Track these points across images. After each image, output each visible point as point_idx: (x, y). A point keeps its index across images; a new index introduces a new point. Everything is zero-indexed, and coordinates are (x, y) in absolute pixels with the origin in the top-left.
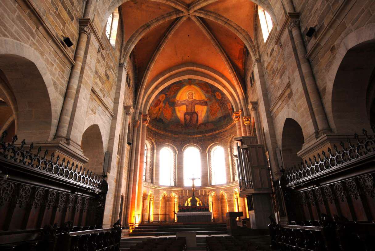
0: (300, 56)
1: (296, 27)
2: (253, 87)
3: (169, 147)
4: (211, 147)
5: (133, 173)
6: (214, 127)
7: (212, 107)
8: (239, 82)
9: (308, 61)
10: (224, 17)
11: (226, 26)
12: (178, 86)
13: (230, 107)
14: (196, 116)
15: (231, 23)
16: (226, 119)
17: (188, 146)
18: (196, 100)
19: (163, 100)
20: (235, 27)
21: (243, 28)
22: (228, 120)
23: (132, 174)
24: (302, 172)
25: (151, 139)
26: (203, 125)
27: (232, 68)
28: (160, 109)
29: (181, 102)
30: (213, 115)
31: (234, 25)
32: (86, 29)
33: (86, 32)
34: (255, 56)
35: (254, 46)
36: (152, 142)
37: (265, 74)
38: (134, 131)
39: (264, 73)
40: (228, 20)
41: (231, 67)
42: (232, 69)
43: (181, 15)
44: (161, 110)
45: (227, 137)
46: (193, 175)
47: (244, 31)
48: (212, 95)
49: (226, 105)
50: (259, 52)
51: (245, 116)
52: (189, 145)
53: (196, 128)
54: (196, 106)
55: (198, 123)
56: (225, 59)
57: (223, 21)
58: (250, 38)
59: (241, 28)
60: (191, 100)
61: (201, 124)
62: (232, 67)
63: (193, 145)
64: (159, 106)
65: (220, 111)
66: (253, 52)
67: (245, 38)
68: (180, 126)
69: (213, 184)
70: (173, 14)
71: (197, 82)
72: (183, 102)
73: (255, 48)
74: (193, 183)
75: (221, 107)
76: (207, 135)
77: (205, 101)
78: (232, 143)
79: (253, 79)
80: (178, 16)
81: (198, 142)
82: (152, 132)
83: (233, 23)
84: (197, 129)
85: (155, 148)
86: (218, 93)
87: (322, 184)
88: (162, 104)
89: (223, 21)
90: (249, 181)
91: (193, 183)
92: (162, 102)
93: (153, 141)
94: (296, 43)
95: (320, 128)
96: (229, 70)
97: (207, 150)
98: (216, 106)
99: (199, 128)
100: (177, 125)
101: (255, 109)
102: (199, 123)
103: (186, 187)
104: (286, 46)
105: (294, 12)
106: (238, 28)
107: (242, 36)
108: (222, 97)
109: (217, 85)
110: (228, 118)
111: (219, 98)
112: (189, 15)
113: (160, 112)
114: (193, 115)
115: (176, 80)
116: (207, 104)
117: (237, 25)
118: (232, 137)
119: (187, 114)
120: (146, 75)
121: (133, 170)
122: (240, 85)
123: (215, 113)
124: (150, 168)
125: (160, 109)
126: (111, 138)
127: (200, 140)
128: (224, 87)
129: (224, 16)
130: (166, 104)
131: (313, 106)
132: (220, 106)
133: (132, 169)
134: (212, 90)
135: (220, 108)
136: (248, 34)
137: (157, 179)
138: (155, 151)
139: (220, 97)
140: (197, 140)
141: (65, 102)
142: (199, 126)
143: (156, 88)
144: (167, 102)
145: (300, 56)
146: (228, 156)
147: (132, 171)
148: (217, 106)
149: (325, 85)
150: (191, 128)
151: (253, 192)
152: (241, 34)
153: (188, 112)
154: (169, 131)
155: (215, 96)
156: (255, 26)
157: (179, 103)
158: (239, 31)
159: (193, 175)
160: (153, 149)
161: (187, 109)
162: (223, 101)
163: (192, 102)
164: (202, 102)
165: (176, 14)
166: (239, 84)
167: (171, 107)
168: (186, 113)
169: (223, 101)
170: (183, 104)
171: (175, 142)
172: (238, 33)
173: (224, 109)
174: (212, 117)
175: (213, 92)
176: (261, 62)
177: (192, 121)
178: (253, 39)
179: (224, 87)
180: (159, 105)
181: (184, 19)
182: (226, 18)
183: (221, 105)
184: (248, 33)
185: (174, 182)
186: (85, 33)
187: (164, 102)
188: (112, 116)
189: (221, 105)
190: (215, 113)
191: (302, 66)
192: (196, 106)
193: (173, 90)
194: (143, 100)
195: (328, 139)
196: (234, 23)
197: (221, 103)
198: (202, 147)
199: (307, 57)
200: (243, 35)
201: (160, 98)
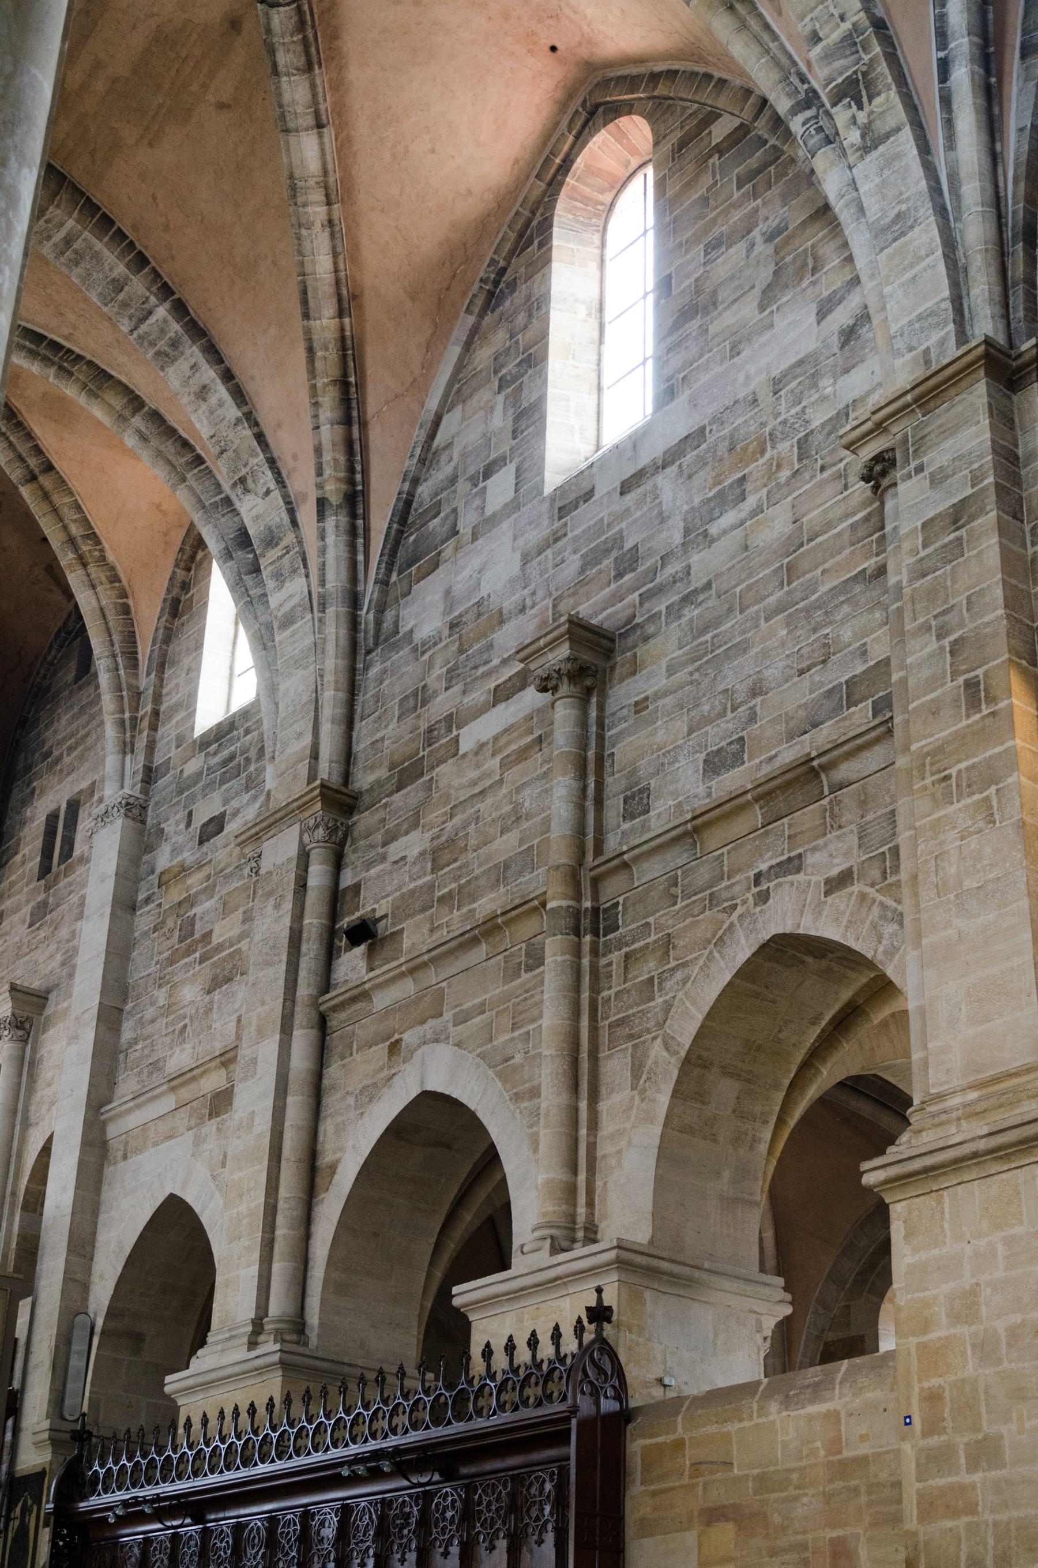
0: (304, 990)
2: (47, 888)
9: (322, 1024)
10: (29, 436)
11: (26, 492)
15: (56, 498)
20: (75, 530)
21: (111, 557)
24: (159, 1460)
31: (69, 515)
34: (124, 753)
35: (137, 695)
39: (141, 897)
40: (49, 468)
47: (115, 578)
50: (151, 747)
57: (22, 459)
58: (131, 638)
59: (102, 551)
66: (121, 723)
67: (106, 623)
73: (137, 710)
79: (69, 843)
83: (68, 500)
87: (213, 1517)
89: (22, 459)
94: (306, 921)
101: (20, 1033)
104: (271, 902)
105: (343, 789)
106: (85, 548)
107: (94, 603)
117: (87, 520)
129: (37, 430)
131: (280, 1220)
136: (126, 610)
149: (338, 1155)
152: (94, 587)
156: (176, 591)
158: (85, 565)
172: (81, 572)
176: (143, 822)
178: (145, 650)
182: (38, 450)
184: (130, 602)
196: (78, 508)
200: (98, 599)
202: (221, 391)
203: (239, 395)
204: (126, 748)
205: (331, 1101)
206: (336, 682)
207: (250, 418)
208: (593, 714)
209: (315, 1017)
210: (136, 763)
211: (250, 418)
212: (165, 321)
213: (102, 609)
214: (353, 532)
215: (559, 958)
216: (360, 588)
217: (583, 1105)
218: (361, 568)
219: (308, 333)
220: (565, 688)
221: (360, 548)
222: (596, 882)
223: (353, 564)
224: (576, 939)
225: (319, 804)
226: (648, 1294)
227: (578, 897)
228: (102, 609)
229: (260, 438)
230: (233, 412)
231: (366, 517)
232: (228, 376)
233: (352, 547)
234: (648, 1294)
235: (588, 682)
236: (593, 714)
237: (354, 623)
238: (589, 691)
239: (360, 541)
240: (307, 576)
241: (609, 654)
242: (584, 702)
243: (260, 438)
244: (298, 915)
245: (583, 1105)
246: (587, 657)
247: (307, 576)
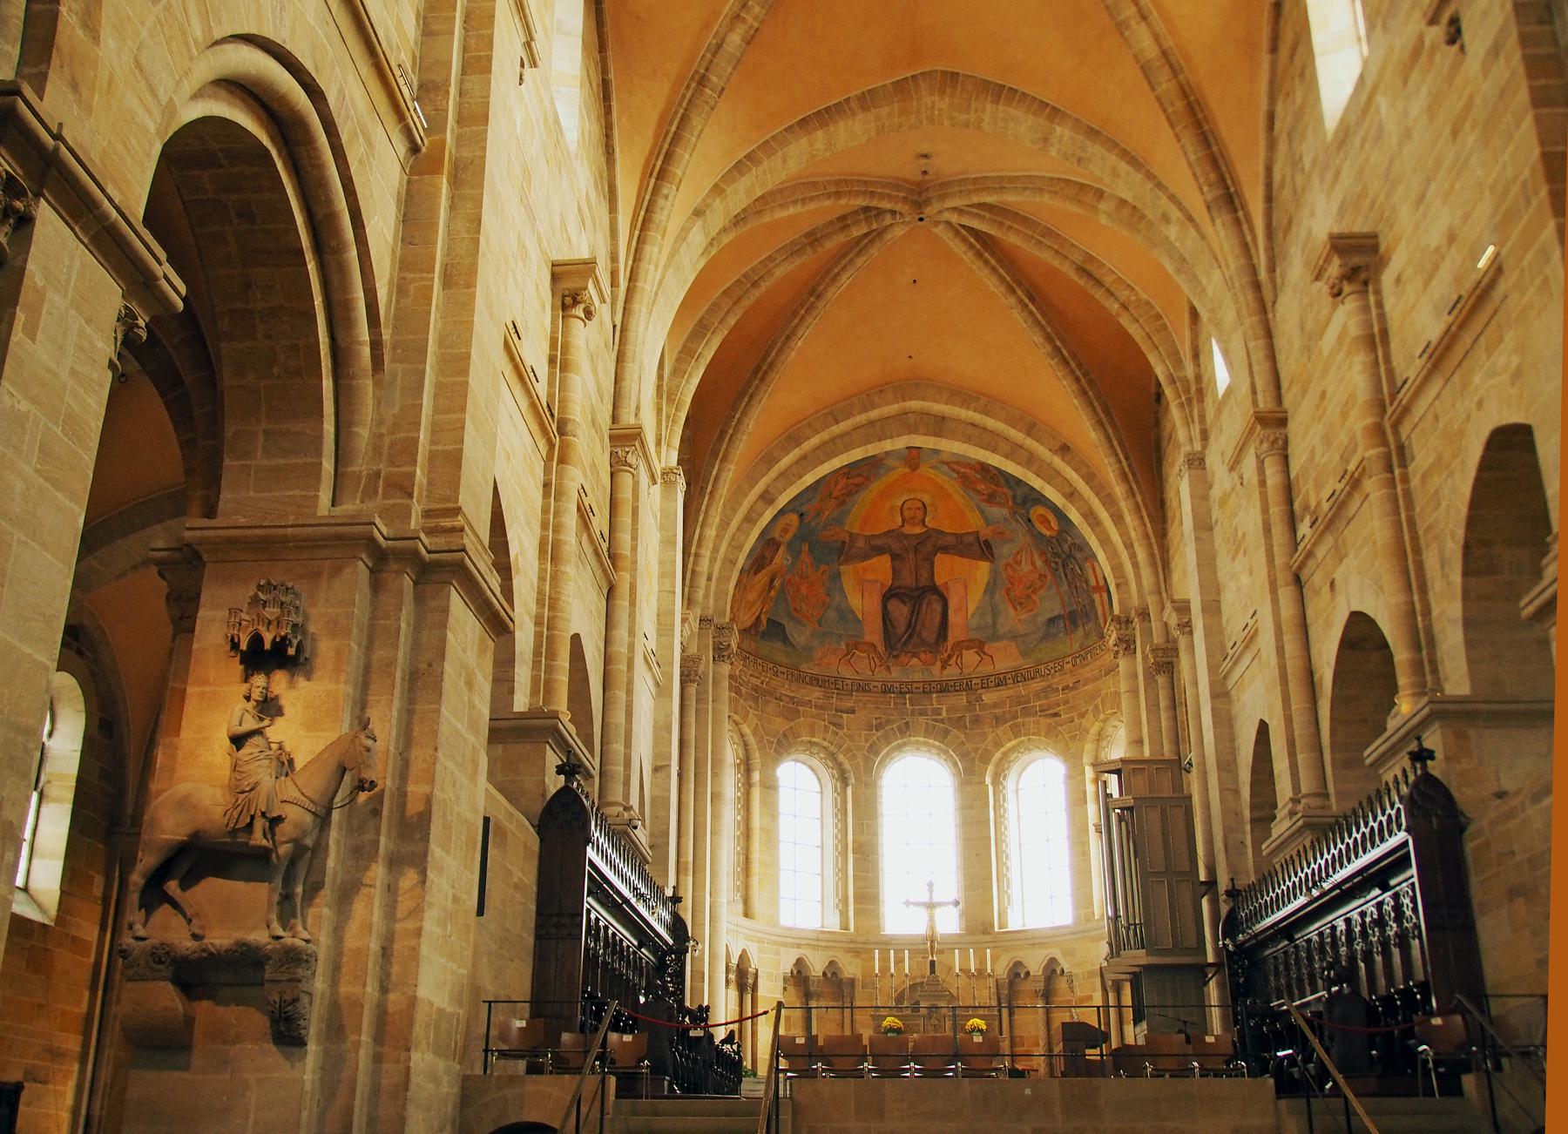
1: (1275, 457)
3: (812, 754)
4: (1005, 754)
5: (690, 878)
6: (1022, 661)
7: (1015, 566)
8: (1135, 488)
12: (860, 475)
13: (1097, 582)
14: (938, 608)
16: (1080, 632)
17: (899, 748)
18: (942, 533)
19: (789, 536)
22: (1087, 636)
23: (686, 881)
24: (1262, 902)
25: (736, 723)
26: (969, 648)
27: (1102, 425)
28: (772, 581)
29: (869, 538)
30: (1021, 604)
32: (631, 459)
33: (630, 466)
35: (1185, 380)
36: (742, 735)
37: (1217, 521)
38: (687, 703)
41: (1100, 423)
43: (888, 220)
44: (777, 583)
45: (1082, 715)
46: (930, 885)
48: (1015, 513)
49: (1081, 570)
52: (905, 744)
53: (939, 664)
54: (940, 559)
55: (945, 638)
56: (1075, 387)
59: (1137, 294)
60: (918, 530)
61: (961, 646)
63: (926, 744)
64: (772, 566)
65: (1054, 591)
68: (865, 655)
69: (1014, 923)
70: (858, 222)
71: (945, 457)
72: (879, 542)
74: (932, 919)
75: (1057, 570)
76: (988, 697)
77: (981, 540)
78: (1104, 743)
80: (875, 226)
81: (947, 732)
82: (744, 690)
84: (943, 668)
85: (757, 760)
86: (1041, 510)
87: (1299, 935)
88: (781, 558)
90: (1131, 922)
91: (932, 919)
92: (782, 549)
93: (746, 729)
95: (1304, 789)
96: (1093, 434)
97: (991, 768)
98: (1033, 564)
99: (952, 661)
100: (847, 645)
102: (951, 641)
103: (893, 937)
108: (1060, 532)
109: (1036, 483)
110: (1091, 625)
111: (1048, 533)
112: (921, 219)
113: (772, 593)
114: (925, 601)
115: (857, 454)
116: (992, 556)
118: (1102, 716)
119: (894, 596)
120: (727, 450)
121: (691, 866)
123: (1029, 597)
124: (738, 853)
125: (772, 581)
126: (660, 764)
127: (959, 723)
128: (1072, 495)
130: (800, 552)
132: (1053, 565)
133: (687, 863)
134: (1014, 498)
135: (1049, 577)
137: (774, 901)
138: (756, 776)
139: (1050, 528)
140: (942, 721)
141: (685, 750)
142: (950, 656)
143: (767, 498)
144: (806, 547)
145: (1279, 561)
146: (1086, 802)
147: (686, 869)
148: (1039, 563)
150: (915, 661)
151: (1144, 961)
153: (900, 588)
154: (816, 681)
155: (1030, 521)
157: (860, 543)
159: (930, 885)
160: (746, 767)
161: (896, 573)
162: (1066, 547)
163: (923, 539)
164: (971, 539)
165: (867, 219)
166: (1134, 496)
167: (823, 567)
168: (890, 590)
169: (1066, 547)
170: (880, 551)
171: (841, 733)
173: (1069, 584)
174: (1012, 611)
175: (1019, 500)
177: (918, 627)
179: (1072, 495)
180: (771, 561)
181: (898, 232)
183: (1056, 563)
185: (837, 912)
186: (623, 470)
187: (789, 545)
188: (657, 684)
189: (1056, 563)
190: (1029, 597)
191: (1280, 592)
192: (940, 559)
193: (834, 495)
194: (713, 560)
195: (1306, 825)
197: (1056, 555)
198: (964, 756)
199: (1293, 569)
201: (776, 534)
202: (1123, 166)
203: (1134, 162)
204: (1188, 422)
205: (1312, 632)
207: (1150, 176)
208: (1372, 299)
209: (1290, 578)
210: (1196, 430)
211: (1150, 176)
212: (1072, 138)
213: (1148, 334)
214: (1238, 222)
215: (1377, 494)
216: (1255, 261)
217: (1416, 598)
218: (1251, 245)
219: (1159, 99)
220: (1347, 288)
222: (1396, 426)
223: (1245, 246)
224: (1389, 475)
225: (1259, 427)
226: (1471, 732)
227: (1385, 443)
228: (1148, 334)
229: (1159, 185)
230: (1138, 177)
231: (1244, 207)
232: (1125, 155)
233: (1241, 232)
234: (1471, 732)
235: (1363, 276)
236: (1372, 299)
237: (1257, 286)
238: (1366, 283)
239: (1245, 226)
240: (1220, 267)
241: (1375, 248)
242: (1363, 293)
243: (1159, 185)
244: (1265, 510)
245: (1416, 598)
246: (1357, 260)
247: (1220, 267)
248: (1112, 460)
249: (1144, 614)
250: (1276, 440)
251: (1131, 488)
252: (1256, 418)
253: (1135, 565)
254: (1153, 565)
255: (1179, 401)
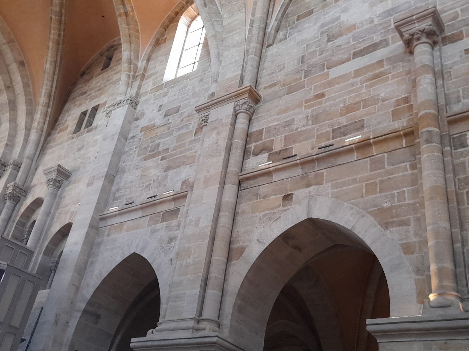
37: (133, 137)
41: (55, 62)
42: (55, 68)
51: (17, 181)
62: (58, 64)
73: (135, 73)
95: (206, 315)
96: (48, 65)
104: (216, 131)
122: (50, 110)
149: (246, 244)
176: (135, 109)
191: (227, 186)
199: (240, 177)
206: (256, 52)
218: (270, 13)
221: (271, 6)
248: (49, 84)
249: (17, 166)
250: (251, 107)
251: (49, 103)
252: (250, 90)
253: (26, 140)
254: (37, 145)
255: (129, 73)
